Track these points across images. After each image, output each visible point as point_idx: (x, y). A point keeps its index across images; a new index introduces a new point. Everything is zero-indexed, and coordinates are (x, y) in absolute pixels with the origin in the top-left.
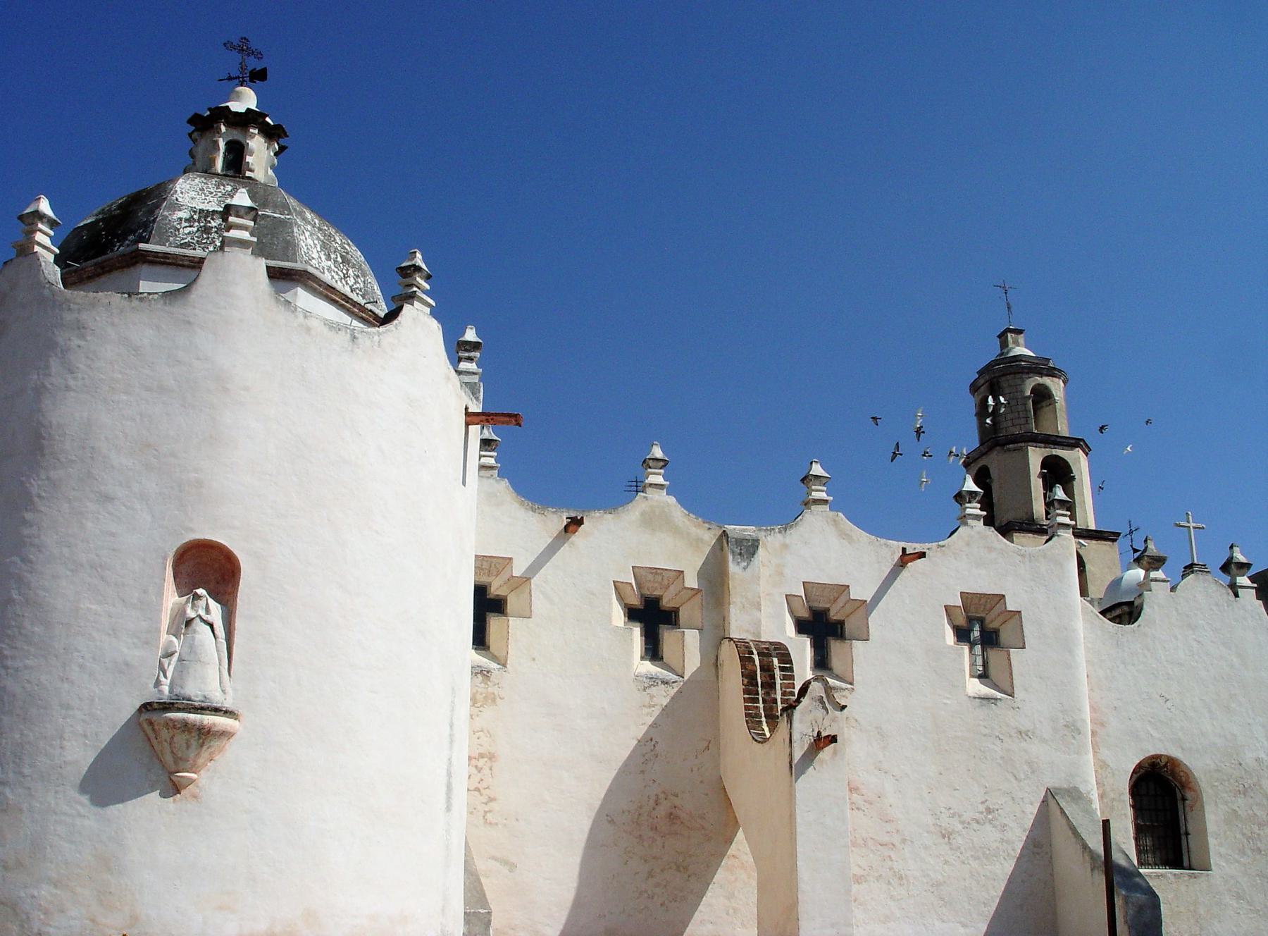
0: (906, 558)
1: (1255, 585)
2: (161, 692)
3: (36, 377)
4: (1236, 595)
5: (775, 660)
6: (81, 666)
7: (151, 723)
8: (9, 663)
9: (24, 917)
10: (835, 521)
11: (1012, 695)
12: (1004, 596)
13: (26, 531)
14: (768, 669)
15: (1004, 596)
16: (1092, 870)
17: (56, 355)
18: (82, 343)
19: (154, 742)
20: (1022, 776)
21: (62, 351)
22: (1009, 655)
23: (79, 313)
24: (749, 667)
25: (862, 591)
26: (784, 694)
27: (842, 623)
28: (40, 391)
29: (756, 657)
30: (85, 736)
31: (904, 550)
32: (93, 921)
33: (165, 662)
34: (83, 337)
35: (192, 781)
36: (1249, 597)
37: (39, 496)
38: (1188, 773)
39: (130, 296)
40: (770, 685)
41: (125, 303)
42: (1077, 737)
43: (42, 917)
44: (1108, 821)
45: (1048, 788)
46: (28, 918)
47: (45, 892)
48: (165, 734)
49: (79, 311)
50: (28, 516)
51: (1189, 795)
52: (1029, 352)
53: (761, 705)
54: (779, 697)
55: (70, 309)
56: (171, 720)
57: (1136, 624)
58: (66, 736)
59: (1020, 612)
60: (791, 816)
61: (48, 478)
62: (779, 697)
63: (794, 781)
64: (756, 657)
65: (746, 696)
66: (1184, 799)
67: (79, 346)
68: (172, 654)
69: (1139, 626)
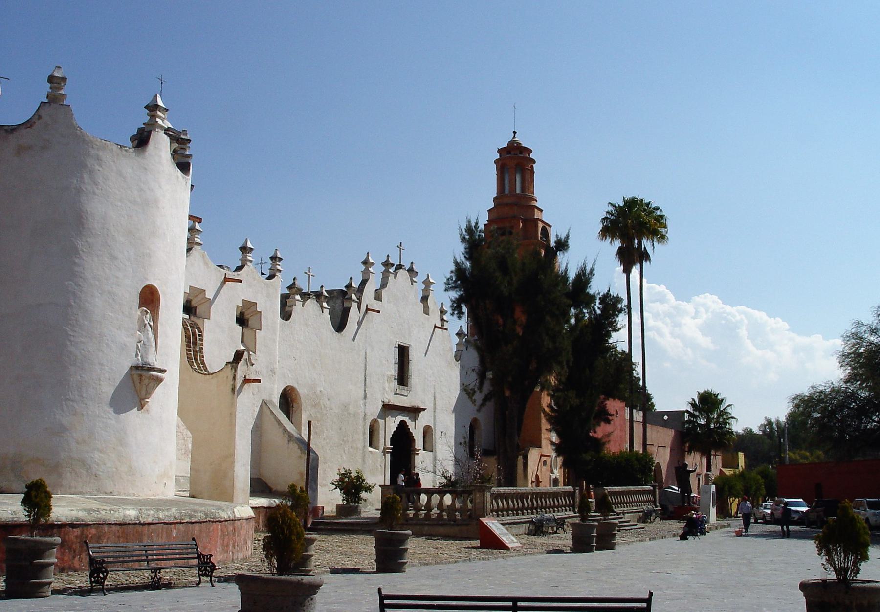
0: (226, 279)
1: (329, 308)
2: (138, 359)
3: (75, 182)
4: (323, 312)
5: (196, 330)
6: (107, 344)
7: (141, 376)
8: (72, 339)
9: (88, 467)
10: (203, 255)
11: (255, 354)
12: (256, 303)
13: (76, 269)
14: (194, 334)
15: (256, 303)
16: (288, 441)
17: (87, 172)
18: (100, 169)
19: (138, 385)
20: (255, 393)
21: (90, 171)
22: (256, 333)
23: (98, 151)
24: (188, 333)
25: (209, 295)
26: (200, 348)
27: (195, 308)
28: (79, 191)
29: (189, 328)
30: (109, 379)
31: (226, 274)
32: (116, 469)
33: (139, 344)
34: (100, 165)
35: (148, 402)
36: (326, 311)
37: (83, 251)
38: (298, 395)
39: (121, 147)
40: (195, 343)
41: (119, 151)
42: (274, 376)
43: (96, 467)
44: (311, 421)
45: (263, 400)
46: (90, 467)
47: (97, 455)
48: (146, 381)
49: (98, 149)
50: (77, 261)
51: (295, 405)
52: (170, 124)
53: (192, 353)
54: (198, 349)
55: (93, 147)
56: (152, 375)
57: (289, 321)
58: (101, 379)
59: (261, 312)
60: (231, 414)
61: (87, 242)
62: (198, 349)
63: (236, 397)
64: (189, 328)
65: (187, 348)
66: (293, 407)
67: (99, 170)
68: (141, 341)
69: (290, 322)
